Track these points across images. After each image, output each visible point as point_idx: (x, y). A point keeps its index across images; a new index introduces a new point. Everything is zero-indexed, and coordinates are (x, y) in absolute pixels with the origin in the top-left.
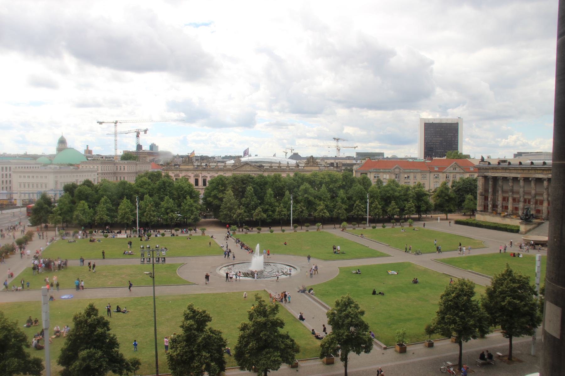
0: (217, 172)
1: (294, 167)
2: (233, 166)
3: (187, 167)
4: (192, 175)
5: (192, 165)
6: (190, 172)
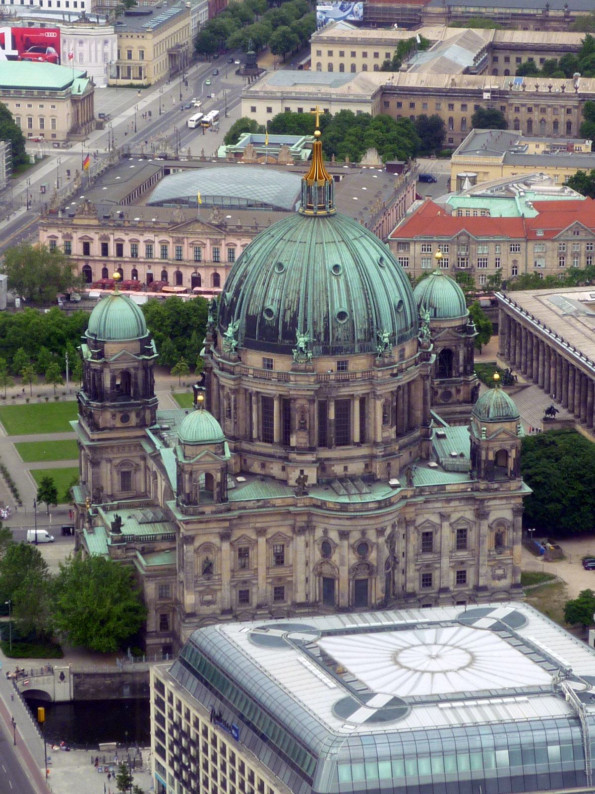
4: (96, 237)
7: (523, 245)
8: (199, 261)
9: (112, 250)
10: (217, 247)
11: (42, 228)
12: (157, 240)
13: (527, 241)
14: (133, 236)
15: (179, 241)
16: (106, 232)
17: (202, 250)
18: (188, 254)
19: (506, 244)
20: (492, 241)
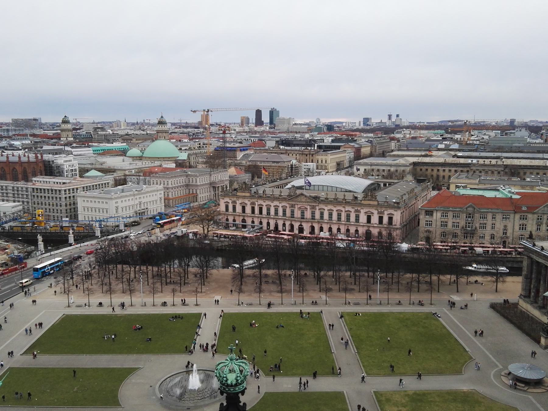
0: (272, 201)
2: (288, 195)
3: (244, 194)
4: (249, 203)
5: (248, 193)
6: (246, 199)
7: (512, 216)
8: (304, 218)
9: (257, 211)
10: (313, 210)
11: (221, 197)
12: (280, 205)
13: (515, 213)
14: (268, 203)
15: (293, 206)
17: (305, 212)
18: (298, 214)
19: (500, 214)
20: (491, 212)
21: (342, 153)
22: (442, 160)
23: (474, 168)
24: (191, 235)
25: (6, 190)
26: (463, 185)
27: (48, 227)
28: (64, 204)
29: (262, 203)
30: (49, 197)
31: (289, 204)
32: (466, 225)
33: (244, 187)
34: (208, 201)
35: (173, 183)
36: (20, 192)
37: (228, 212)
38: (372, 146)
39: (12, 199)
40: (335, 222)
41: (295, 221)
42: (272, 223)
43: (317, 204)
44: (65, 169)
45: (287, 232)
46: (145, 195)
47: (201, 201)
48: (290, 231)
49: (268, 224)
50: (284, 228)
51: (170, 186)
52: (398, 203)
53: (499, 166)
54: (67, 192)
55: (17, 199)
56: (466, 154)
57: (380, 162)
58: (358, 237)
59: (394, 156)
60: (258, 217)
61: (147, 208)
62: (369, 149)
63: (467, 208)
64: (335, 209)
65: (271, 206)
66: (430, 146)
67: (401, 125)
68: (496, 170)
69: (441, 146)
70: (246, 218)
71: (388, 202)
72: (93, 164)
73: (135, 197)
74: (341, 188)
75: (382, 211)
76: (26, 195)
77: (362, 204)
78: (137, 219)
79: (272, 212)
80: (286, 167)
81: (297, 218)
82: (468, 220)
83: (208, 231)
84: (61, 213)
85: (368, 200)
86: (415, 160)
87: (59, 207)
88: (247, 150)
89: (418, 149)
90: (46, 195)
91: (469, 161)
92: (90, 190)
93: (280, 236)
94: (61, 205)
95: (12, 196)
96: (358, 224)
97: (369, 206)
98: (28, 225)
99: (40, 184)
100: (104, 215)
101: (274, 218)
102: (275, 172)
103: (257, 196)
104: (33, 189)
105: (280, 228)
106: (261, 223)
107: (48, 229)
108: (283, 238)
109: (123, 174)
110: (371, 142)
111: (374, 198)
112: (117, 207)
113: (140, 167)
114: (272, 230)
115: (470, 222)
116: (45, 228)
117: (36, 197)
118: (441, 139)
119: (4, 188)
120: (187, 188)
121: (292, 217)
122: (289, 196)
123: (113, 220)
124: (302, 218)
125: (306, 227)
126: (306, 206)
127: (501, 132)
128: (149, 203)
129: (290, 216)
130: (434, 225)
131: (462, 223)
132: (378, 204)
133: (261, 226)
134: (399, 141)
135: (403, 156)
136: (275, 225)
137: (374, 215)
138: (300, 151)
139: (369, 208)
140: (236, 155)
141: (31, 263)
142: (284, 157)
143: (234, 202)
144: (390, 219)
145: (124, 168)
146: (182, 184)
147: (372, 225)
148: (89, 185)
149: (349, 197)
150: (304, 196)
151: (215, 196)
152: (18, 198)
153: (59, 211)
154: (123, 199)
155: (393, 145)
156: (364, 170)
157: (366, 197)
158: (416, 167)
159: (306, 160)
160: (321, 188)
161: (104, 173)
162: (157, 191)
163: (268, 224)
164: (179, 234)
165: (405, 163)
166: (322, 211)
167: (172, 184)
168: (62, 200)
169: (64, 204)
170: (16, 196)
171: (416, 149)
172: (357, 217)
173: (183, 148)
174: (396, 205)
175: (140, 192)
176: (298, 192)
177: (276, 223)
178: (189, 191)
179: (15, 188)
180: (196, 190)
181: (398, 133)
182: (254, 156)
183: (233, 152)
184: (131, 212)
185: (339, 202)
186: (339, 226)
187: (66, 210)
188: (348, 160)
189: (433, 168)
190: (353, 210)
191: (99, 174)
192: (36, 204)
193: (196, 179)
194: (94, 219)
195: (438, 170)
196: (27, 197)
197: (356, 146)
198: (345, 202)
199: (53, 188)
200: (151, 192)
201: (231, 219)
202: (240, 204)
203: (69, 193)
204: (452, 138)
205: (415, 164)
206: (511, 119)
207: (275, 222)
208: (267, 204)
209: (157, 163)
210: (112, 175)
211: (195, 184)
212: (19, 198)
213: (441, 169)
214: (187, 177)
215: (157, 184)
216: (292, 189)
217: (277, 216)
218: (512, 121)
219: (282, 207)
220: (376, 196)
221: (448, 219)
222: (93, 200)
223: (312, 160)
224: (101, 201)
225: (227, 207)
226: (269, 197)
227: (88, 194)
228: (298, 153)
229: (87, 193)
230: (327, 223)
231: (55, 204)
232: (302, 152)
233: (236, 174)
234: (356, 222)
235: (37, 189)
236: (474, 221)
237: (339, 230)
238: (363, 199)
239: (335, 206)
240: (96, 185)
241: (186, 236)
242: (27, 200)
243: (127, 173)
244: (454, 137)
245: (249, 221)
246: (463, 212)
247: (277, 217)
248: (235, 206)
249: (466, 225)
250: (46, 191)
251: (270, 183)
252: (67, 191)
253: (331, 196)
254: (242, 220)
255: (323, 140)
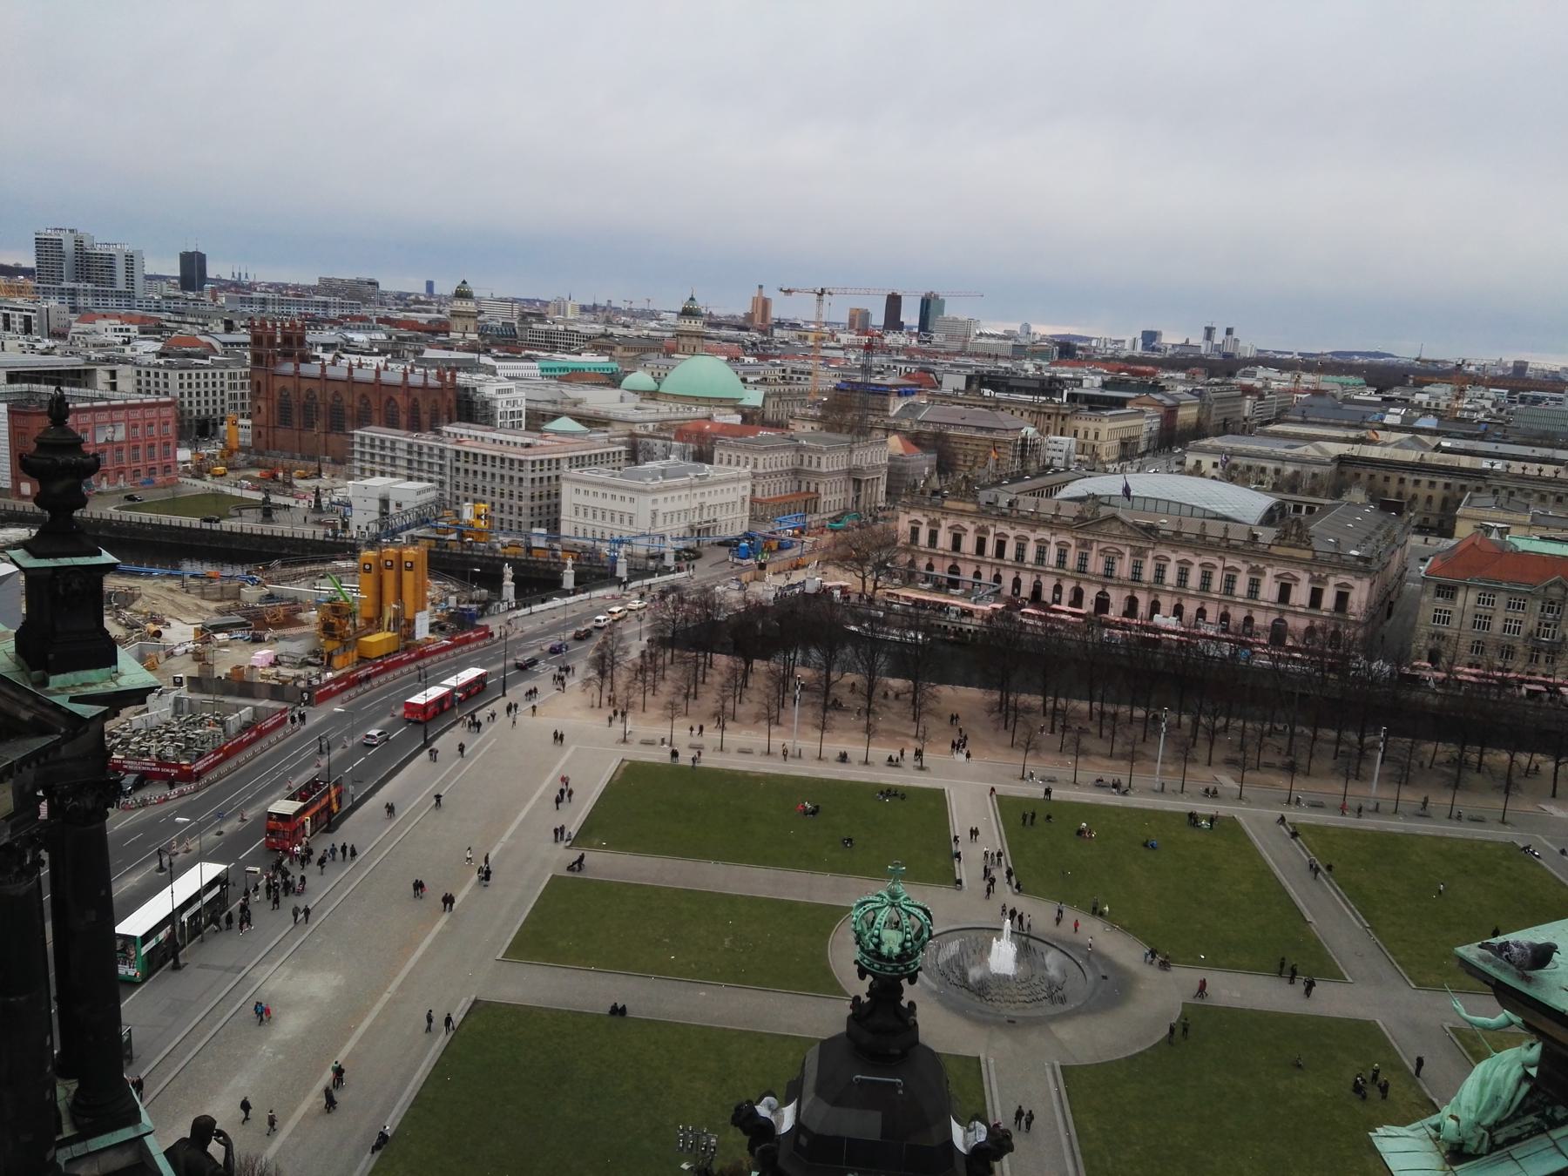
0: (1033, 528)
1: (1240, 543)
2: (1077, 517)
3: (960, 506)
4: (971, 528)
5: (973, 503)
6: (966, 519)
8: (1111, 577)
11: (903, 509)
12: (1053, 540)
14: (1021, 531)
15: (1085, 544)
16: (986, 523)
17: (1117, 562)
18: (1096, 564)
21: (1134, 418)
22: (1414, 456)
23: (1496, 483)
24: (837, 593)
25: (393, 449)
26: (1499, 525)
27: (499, 546)
28: (527, 494)
29: (1005, 532)
30: (493, 475)
31: (1077, 538)
32: (1539, 630)
33: (963, 488)
34: (838, 513)
35: (767, 465)
36: (425, 458)
37: (916, 545)
38: (1202, 405)
39: (406, 472)
40: (1241, 600)
41: (1088, 581)
42: (1027, 581)
43: (1151, 545)
44: (500, 410)
45: (1064, 607)
46: (712, 489)
47: (825, 513)
48: (1071, 604)
49: (1017, 583)
50: (1057, 596)
51: (760, 470)
52: (1367, 560)
53: (1528, 479)
54: (538, 467)
55: (416, 474)
56: (1462, 444)
57: (1255, 447)
58: (1250, 636)
59: (1276, 435)
60: (992, 564)
61: (715, 520)
62: (1196, 411)
63: (1546, 588)
64: (1197, 561)
65: (1028, 540)
66: (1364, 417)
67: (1237, 353)
68: (1551, 493)
69: (1388, 420)
70: (959, 564)
71: (1340, 555)
72: (555, 402)
73: (694, 491)
74: (1205, 510)
75: (1323, 575)
76: (440, 465)
77: (1271, 554)
78: (692, 544)
79: (1031, 554)
80: (1010, 443)
81: (1094, 575)
82: (1545, 618)
83: (876, 588)
84: (520, 515)
85: (1290, 546)
86: (1344, 449)
87: (515, 501)
88: (913, 393)
89: (1331, 421)
90: (488, 469)
91: (1485, 464)
92: (583, 465)
93: (1052, 615)
94: (520, 497)
95: (406, 465)
96: (1255, 602)
97: (1290, 560)
98: (453, 536)
99: (475, 444)
100: (615, 527)
101: (1033, 571)
102: (981, 454)
103: (994, 513)
104: (458, 452)
105: (1047, 595)
106: (998, 578)
107: (496, 551)
108: (1063, 621)
109: (627, 432)
110: (1200, 394)
111: (1304, 540)
112: (654, 513)
113: (666, 416)
114: (1026, 599)
115: (1549, 622)
116: (490, 548)
117: (462, 471)
118: (1380, 399)
119: (388, 444)
120: (796, 478)
121: (1080, 572)
122: (1080, 518)
123: (645, 541)
124: (1106, 576)
125: (1117, 599)
126: (1121, 549)
127: (1509, 394)
128: (718, 508)
129: (1075, 567)
130: (1455, 623)
131: (1531, 623)
132: (1315, 558)
133: (999, 587)
134: (1261, 397)
135: (1311, 439)
136: (1034, 586)
137: (1300, 583)
138: (1034, 406)
139: (1288, 567)
140: (888, 405)
141: (494, 624)
142: (1005, 418)
143: (934, 524)
144: (1342, 598)
145: (630, 418)
146: (785, 468)
147: (1292, 609)
148: (584, 453)
149: (1238, 535)
150: (1119, 523)
151: (857, 502)
152: (419, 470)
153: (515, 510)
154: (669, 495)
155: (1247, 406)
156: (1194, 463)
157: (1284, 539)
158: (1343, 469)
159: (1048, 428)
160: (1162, 507)
161: (586, 426)
162: (739, 480)
163: (1017, 583)
164: (811, 588)
165: (1319, 454)
166: (1162, 562)
167: (764, 467)
168: (524, 484)
169: (529, 494)
170: (415, 465)
171: (1326, 421)
172: (1254, 587)
173: (751, 379)
174: (1360, 563)
175: (703, 481)
176: (1104, 511)
177: (1038, 581)
178: (800, 487)
179: (416, 449)
180: (817, 484)
181: (1245, 375)
182: (930, 413)
183: (881, 397)
184: (680, 527)
185: (1211, 544)
186: (1203, 603)
187: (532, 509)
188: (1145, 436)
189: (1388, 474)
190: (1244, 568)
191: (578, 427)
192: (462, 487)
193: (819, 458)
194: (607, 537)
195: (1402, 481)
196: (441, 469)
197: (1168, 402)
198: (1226, 546)
199: (505, 455)
200: (727, 481)
201: (922, 564)
202: (949, 528)
203: (541, 470)
204: (1407, 400)
205: (1342, 460)
206: (1515, 362)
207: (1035, 578)
208: (1019, 533)
209: (702, 411)
210: (605, 432)
211: (817, 470)
212: (422, 470)
213: (1409, 478)
214: (797, 451)
215: (729, 462)
216: (1089, 501)
217: (1042, 565)
218: (1520, 367)
219: (1058, 544)
220: (1309, 538)
221: (1495, 609)
222: (600, 491)
223: (1062, 429)
224: (618, 494)
225: (915, 532)
226: (1024, 517)
227: (586, 474)
228: (1026, 410)
229: (585, 473)
230: (1173, 593)
231: (506, 492)
232: (1040, 407)
233: (902, 452)
234: (1250, 597)
235: (467, 454)
236: (1560, 620)
237: (1201, 613)
238: (1276, 542)
239: (1198, 552)
240: (596, 456)
241: (825, 592)
242: (441, 477)
243: (638, 429)
244: (1411, 399)
245: (967, 572)
246: (1534, 596)
247: (1040, 568)
248: (936, 531)
249: (1539, 630)
250: (489, 461)
251: (1010, 483)
252: (538, 463)
253: (1191, 528)
254: (951, 567)
255: (1081, 381)
